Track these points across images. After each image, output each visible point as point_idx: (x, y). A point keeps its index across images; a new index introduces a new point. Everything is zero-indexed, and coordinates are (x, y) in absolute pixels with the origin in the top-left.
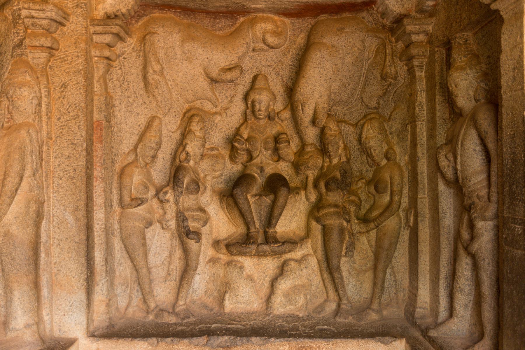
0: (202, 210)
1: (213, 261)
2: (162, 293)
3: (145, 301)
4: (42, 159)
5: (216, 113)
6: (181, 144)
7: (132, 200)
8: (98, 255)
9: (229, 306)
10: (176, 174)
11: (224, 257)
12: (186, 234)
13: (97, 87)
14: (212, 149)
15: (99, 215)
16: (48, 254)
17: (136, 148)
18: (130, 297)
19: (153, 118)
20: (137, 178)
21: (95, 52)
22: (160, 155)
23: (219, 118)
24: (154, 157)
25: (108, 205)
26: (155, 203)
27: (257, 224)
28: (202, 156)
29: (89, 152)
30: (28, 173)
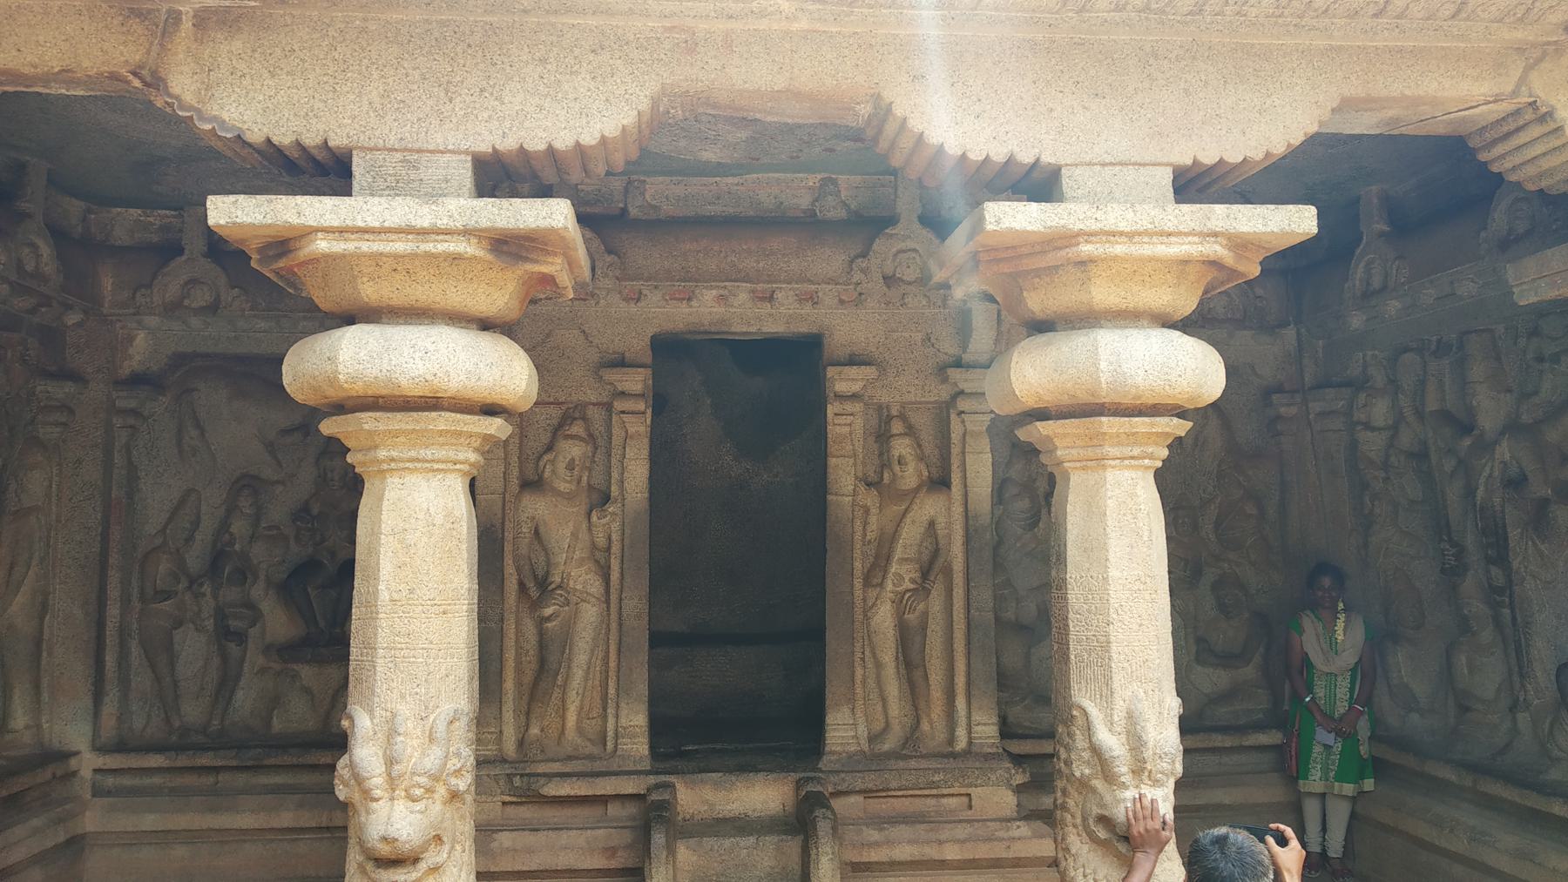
0: (250, 605)
1: (263, 671)
2: (192, 711)
3: (168, 720)
4: (48, 545)
5: (278, 482)
6: (224, 526)
7: (156, 592)
8: (110, 659)
9: (277, 725)
10: (217, 558)
11: (277, 666)
12: (227, 635)
13: (118, 459)
14: (269, 528)
15: (113, 611)
16: (50, 654)
17: (165, 528)
18: (149, 716)
19: (189, 491)
20: (164, 566)
21: (118, 421)
22: (198, 536)
23: (281, 488)
24: (190, 539)
25: (126, 600)
26: (188, 597)
27: (322, 624)
28: (253, 538)
29: (105, 537)
30: (34, 562)
